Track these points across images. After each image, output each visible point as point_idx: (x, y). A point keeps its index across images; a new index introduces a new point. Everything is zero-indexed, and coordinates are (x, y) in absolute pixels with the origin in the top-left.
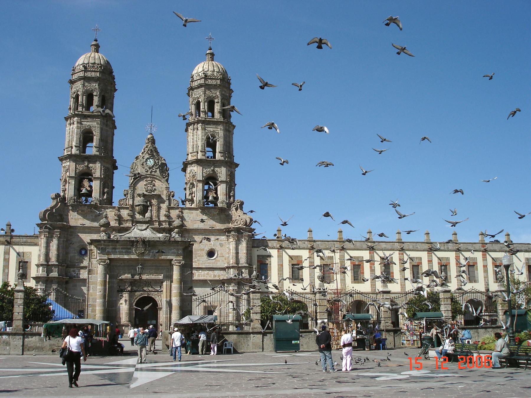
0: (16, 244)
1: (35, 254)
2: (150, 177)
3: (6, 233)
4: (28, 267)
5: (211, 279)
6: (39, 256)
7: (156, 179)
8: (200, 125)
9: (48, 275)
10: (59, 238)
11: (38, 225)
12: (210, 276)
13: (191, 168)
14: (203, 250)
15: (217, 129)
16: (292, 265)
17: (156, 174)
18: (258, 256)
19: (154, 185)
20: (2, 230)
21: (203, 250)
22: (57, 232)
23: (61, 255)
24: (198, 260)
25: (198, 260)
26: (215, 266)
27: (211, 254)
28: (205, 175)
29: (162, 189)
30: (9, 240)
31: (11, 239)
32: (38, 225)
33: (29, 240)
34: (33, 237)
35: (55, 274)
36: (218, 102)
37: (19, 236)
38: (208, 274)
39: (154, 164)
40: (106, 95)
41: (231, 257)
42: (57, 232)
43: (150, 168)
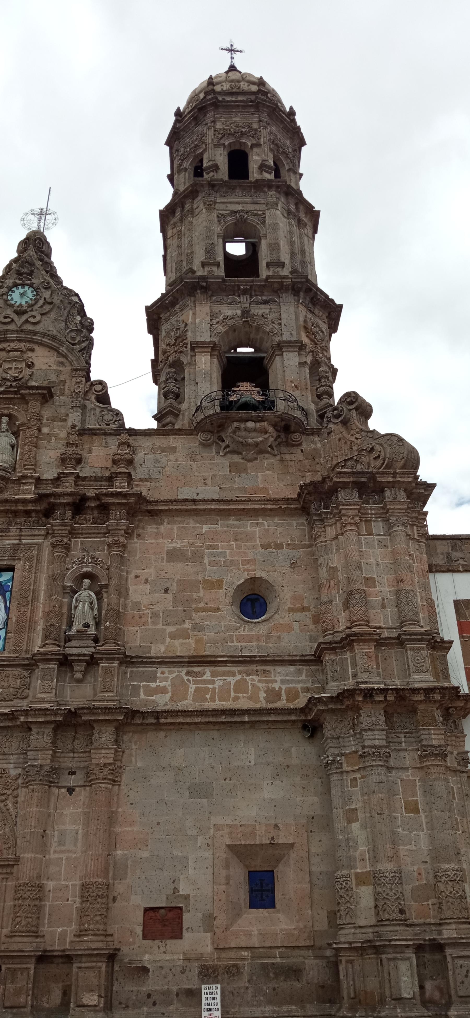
2: (20, 341)
5: (257, 706)
7: (41, 344)
8: (199, 203)
12: (257, 700)
13: (173, 320)
14: (219, 584)
15: (257, 207)
17: (38, 328)
18: (457, 604)
19: (30, 365)
21: (219, 584)
24: (198, 628)
25: (198, 628)
26: (271, 649)
27: (253, 602)
28: (221, 329)
29: (62, 377)
36: (258, 145)
38: (240, 687)
39: (37, 301)
41: (338, 602)
43: (20, 312)
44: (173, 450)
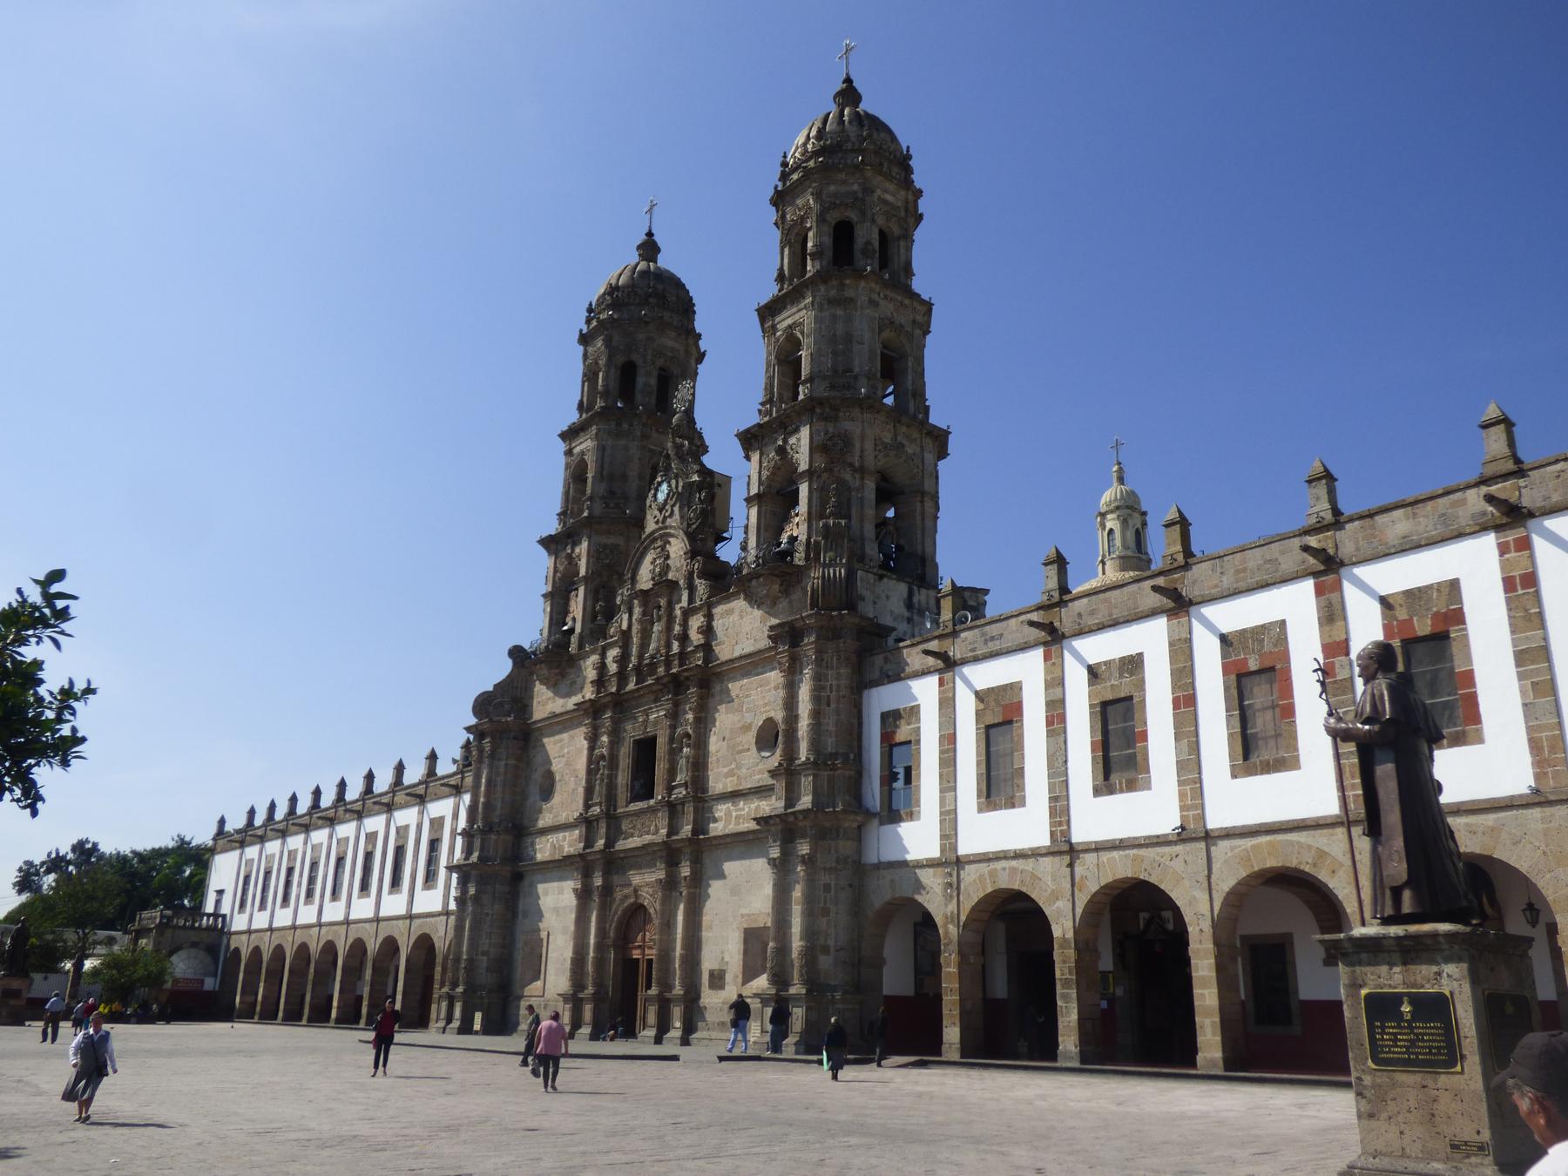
16: (988, 728)
19: (668, 557)
21: (747, 728)
23: (499, 805)
24: (739, 767)
40: (634, 357)
44: (731, 612)
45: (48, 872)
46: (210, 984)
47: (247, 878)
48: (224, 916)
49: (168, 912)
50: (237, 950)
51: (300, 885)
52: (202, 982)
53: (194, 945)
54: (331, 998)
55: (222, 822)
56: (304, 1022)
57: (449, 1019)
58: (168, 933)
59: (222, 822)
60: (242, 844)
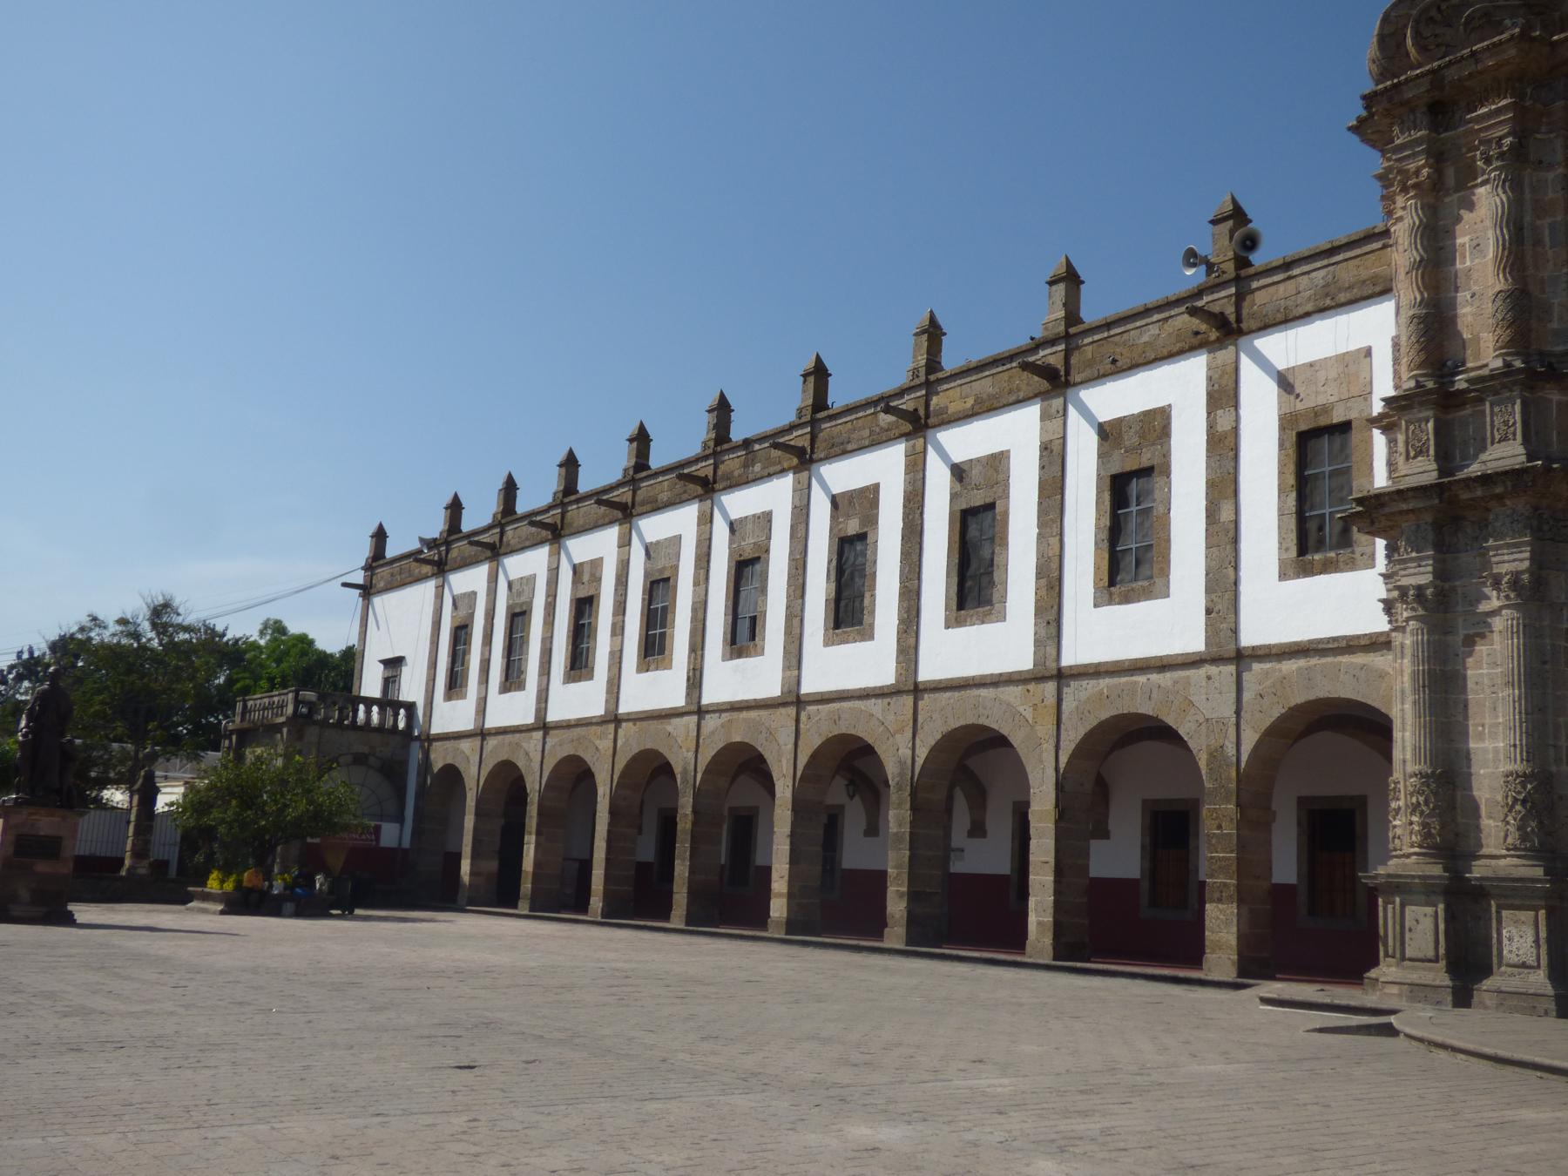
0: (1269, 325)
1: (1366, 339)
3: (1210, 267)
4: (1356, 457)
6: (1396, 346)
9: (1446, 459)
10: (1519, 162)
11: (1359, 129)
20: (1191, 258)
22: (1492, 120)
30: (1230, 311)
31: (1240, 298)
32: (1359, 129)
33: (1349, 270)
34: (1369, 237)
35: (1506, 454)
37: (1287, 266)
42: (1492, 120)
45: (20, 678)
46: (391, 835)
47: (461, 633)
48: (410, 707)
49: (310, 695)
50: (452, 775)
51: (618, 630)
52: (378, 829)
53: (359, 760)
54: (586, 866)
55: (380, 536)
56: (677, 921)
57: (1468, 963)
58: (312, 733)
59: (380, 536)
60: (441, 568)
